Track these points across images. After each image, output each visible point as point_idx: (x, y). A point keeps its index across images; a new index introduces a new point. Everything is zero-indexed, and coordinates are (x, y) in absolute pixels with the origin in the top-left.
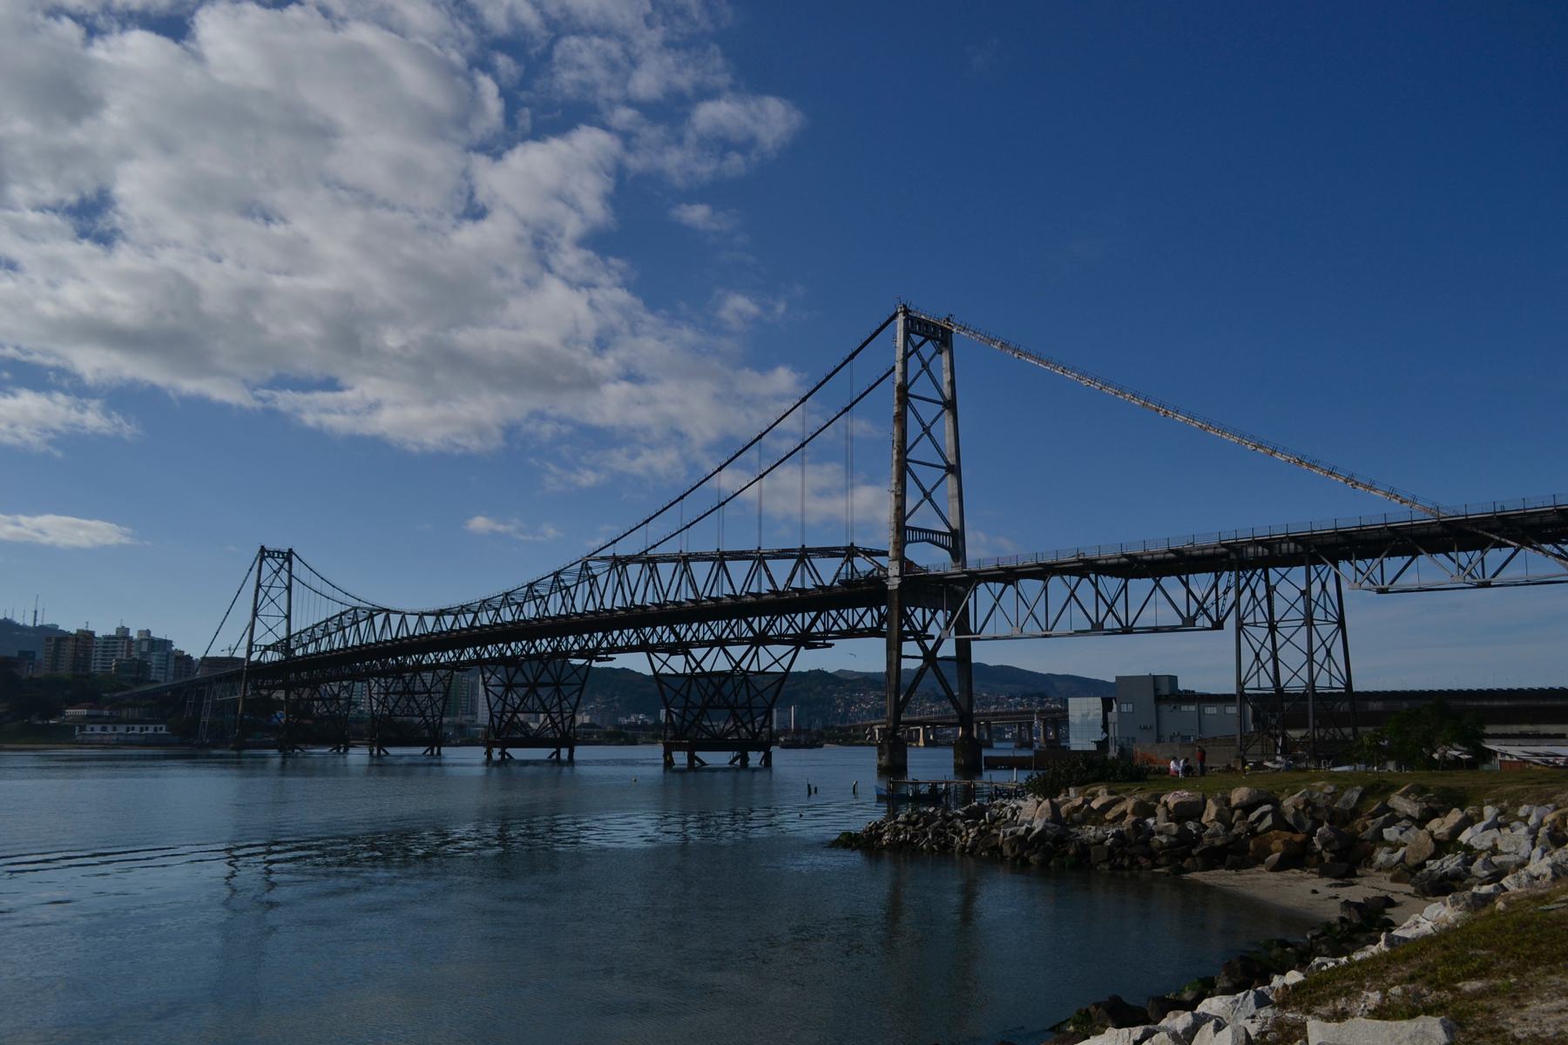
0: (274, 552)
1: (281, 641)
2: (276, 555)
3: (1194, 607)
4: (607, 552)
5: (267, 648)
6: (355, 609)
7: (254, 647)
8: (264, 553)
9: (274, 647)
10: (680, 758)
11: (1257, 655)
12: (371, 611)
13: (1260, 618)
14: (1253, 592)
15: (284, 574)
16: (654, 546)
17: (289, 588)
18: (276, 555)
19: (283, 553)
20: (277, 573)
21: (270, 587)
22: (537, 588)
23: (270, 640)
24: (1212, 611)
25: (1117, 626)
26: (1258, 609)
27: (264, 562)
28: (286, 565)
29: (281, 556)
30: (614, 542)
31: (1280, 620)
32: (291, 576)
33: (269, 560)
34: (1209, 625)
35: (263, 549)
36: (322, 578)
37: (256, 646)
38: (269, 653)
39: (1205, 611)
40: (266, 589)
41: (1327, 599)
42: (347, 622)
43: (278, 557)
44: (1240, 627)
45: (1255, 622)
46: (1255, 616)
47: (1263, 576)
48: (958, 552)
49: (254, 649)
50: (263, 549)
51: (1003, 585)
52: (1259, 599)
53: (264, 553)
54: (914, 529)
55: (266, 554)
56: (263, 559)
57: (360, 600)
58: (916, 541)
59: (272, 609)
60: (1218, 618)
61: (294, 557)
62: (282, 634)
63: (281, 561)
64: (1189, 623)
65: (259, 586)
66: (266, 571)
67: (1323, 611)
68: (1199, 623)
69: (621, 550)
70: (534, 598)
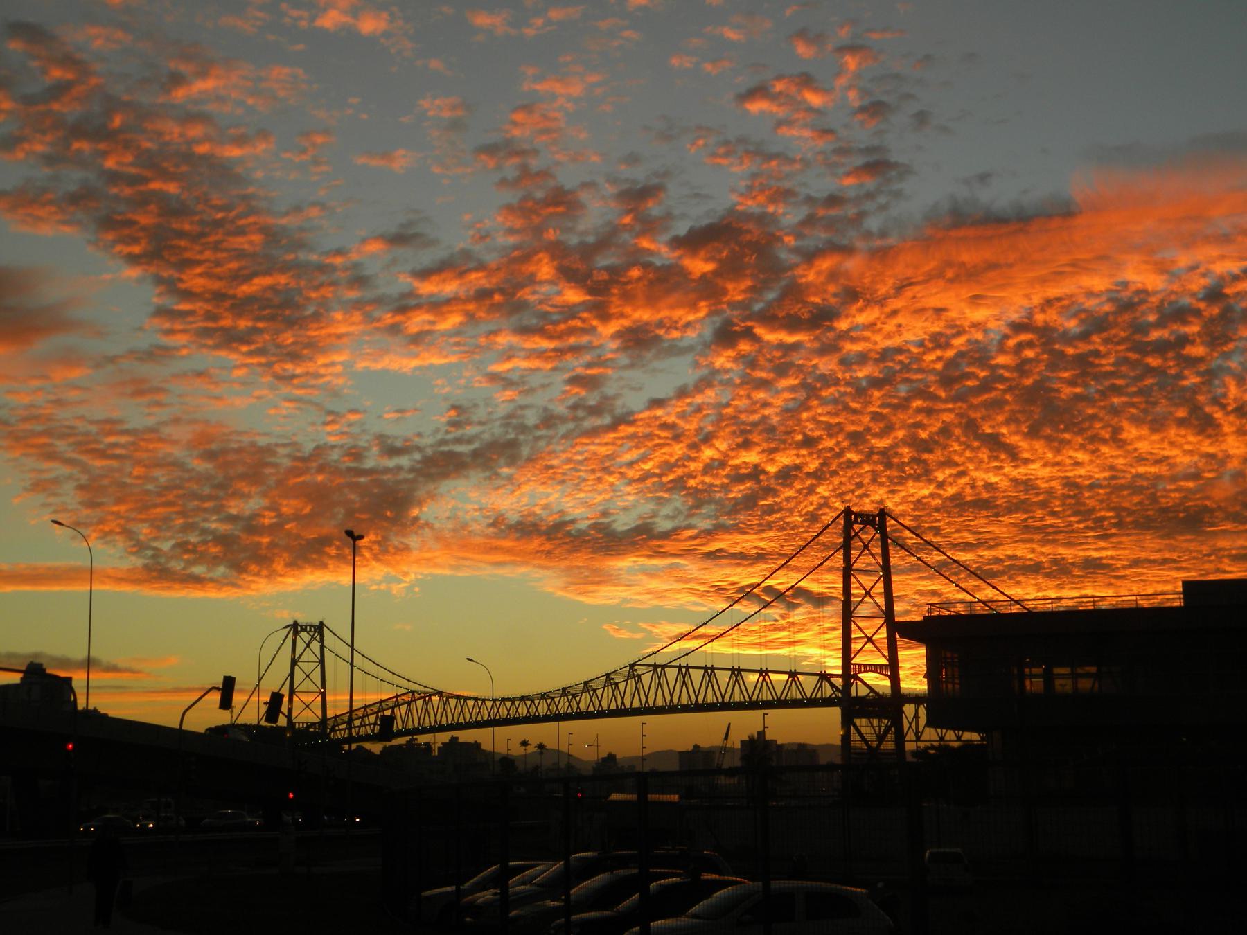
0: (306, 626)
2: (308, 628)
4: (650, 661)
6: (413, 692)
15: (315, 646)
17: (322, 662)
18: (308, 628)
19: (314, 627)
20: (308, 645)
27: (298, 637)
28: (318, 638)
29: (313, 629)
32: (322, 647)
48: (895, 679)
50: (295, 625)
53: (296, 628)
54: (859, 665)
56: (296, 633)
57: (409, 681)
59: (307, 685)
61: (325, 629)
70: (589, 691)
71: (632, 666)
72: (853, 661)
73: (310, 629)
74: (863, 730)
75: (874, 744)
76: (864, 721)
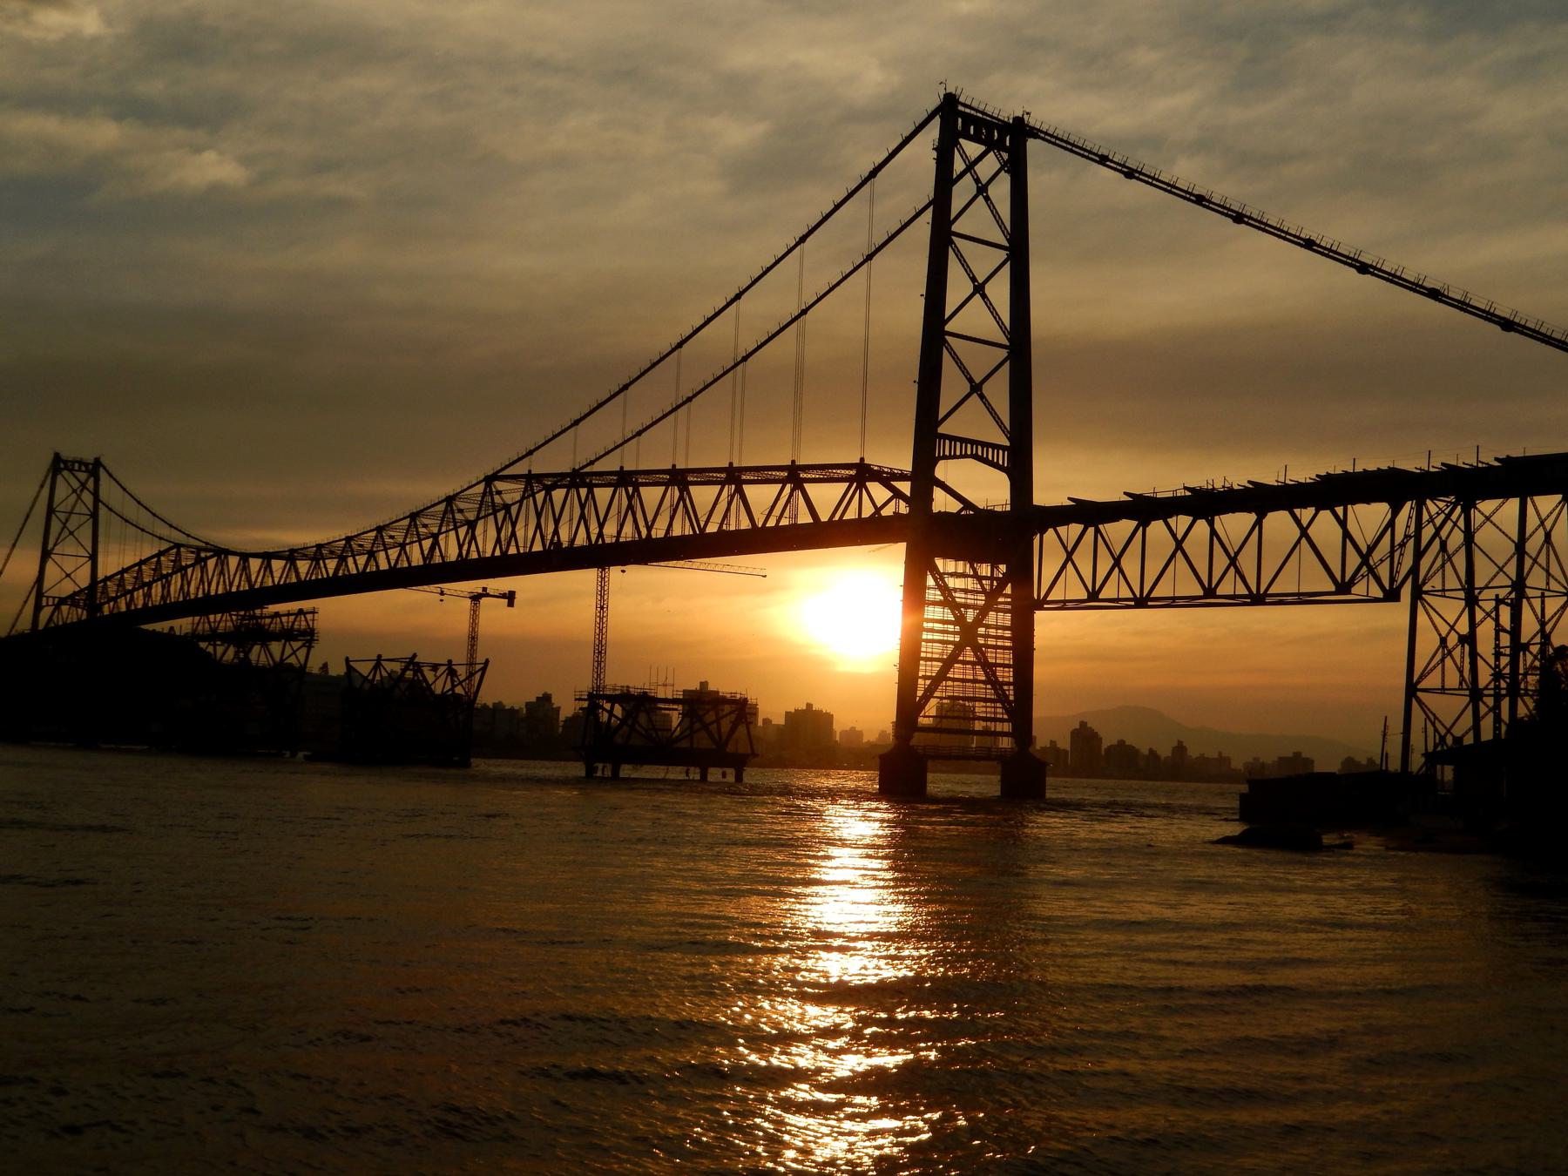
0: (73, 462)
1: (82, 590)
2: (77, 465)
3: (1353, 560)
5: (62, 601)
6: (178, 546)
7: (44, 599)
8: (59, 465)
9: (71, 600)
10: (602, 770)
11: (1443, 641)
12: (199, 550)
13: (1452, 583)
14: (1443, 545)
16: (592, 463)
17: (94, 516)
18: (77, 465)
19: (86, 465)
21: (71, 513)
22: (426, 521)
23: (68, 588)
24: (1383, 571)
25: (1242, 590)
26: (1448, 566)
27: (59, 478)
28: (90, 484)
29: (83, 468)
30: (530, 453)
31: (1487, 587)
33: (65, 473)
34: (1380, 595)
35: (57, 458)
36: (139, 503)
37: (48, 597)
38: (65, 608)
39: (1372, 571)
40: (63, 516)
41: (1551, 552)
42: (167, 564)
43: (80, 470)
44: (1417, 594)
45: (1444, 590)
46: (1443, 578)
47: (1461, 523)
49: (44, 603)
50: (57, 458)
51: (1081, 527)
52: (1450, 552)
53: (59, 465)
54: (953, 439)
55: (62, 466)
58: (955, 457)
60: (1392, 579)
61: (101, 470)
62: (83, 579)
63: (83, 476)
64: (1344, 587)
65: (51, 511)
66: (62, 491)
67: (1544, 574)
68: (1359, 589)
69: (542, 464)
71: (489, 480)
72: (941, 430)
73: (80, 467)
74: (952, 582)
75: (970, 615)
76: (961, 566)
